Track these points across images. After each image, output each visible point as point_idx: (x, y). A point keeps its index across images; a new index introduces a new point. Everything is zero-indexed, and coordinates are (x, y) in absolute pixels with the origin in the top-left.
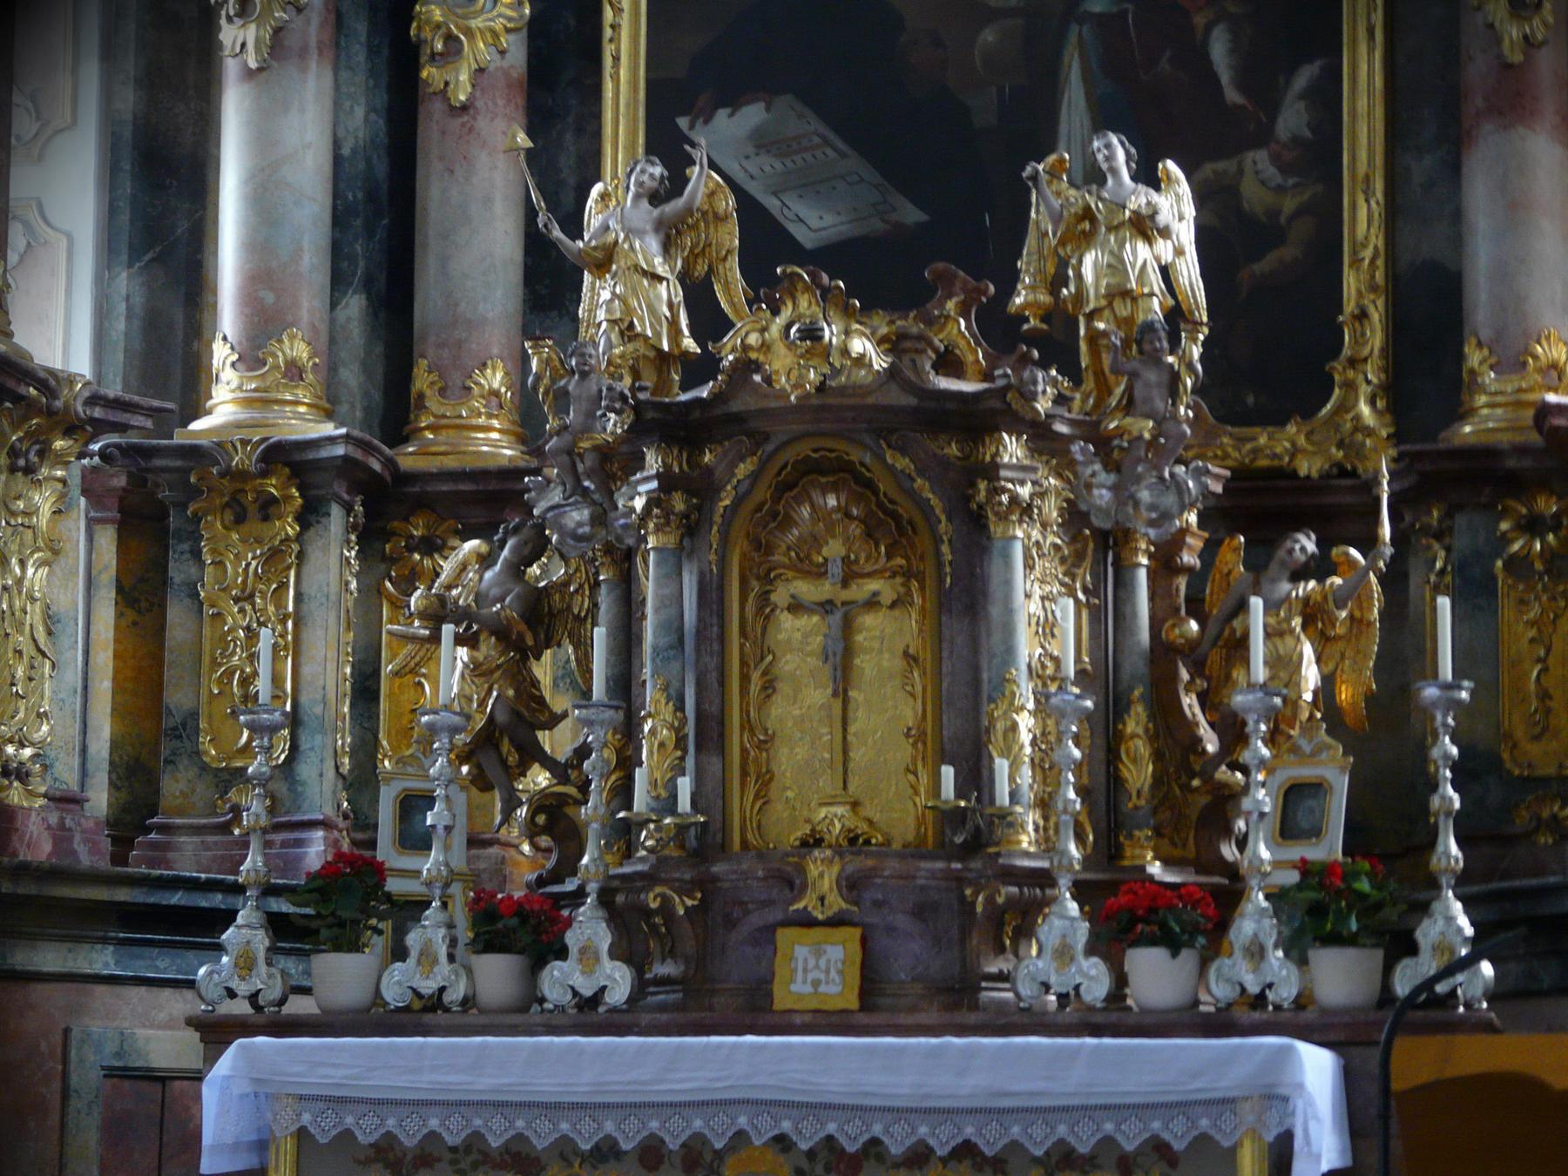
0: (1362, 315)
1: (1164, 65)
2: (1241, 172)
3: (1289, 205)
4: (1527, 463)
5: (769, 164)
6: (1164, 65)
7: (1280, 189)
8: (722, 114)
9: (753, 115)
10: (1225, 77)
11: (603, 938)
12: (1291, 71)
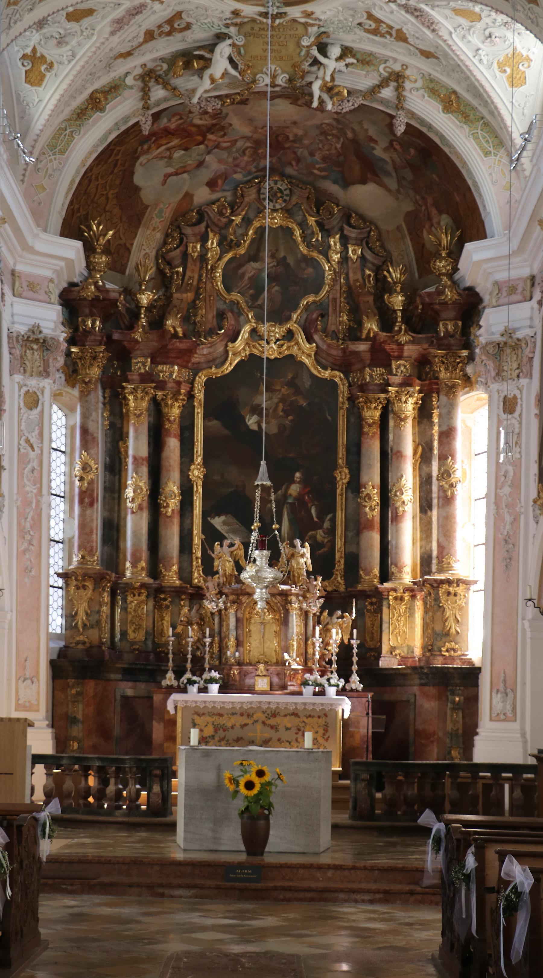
0: (339, 562)
1: (303, 513)
3: (326, 540)
4: (371, 593)
5: (226, 528)
6: (303, 513)
7: (324, 537)
8: (217, 518)
9: (223, 518)
10: (314, 516)
11: (173, 676)
12: (327, 515)
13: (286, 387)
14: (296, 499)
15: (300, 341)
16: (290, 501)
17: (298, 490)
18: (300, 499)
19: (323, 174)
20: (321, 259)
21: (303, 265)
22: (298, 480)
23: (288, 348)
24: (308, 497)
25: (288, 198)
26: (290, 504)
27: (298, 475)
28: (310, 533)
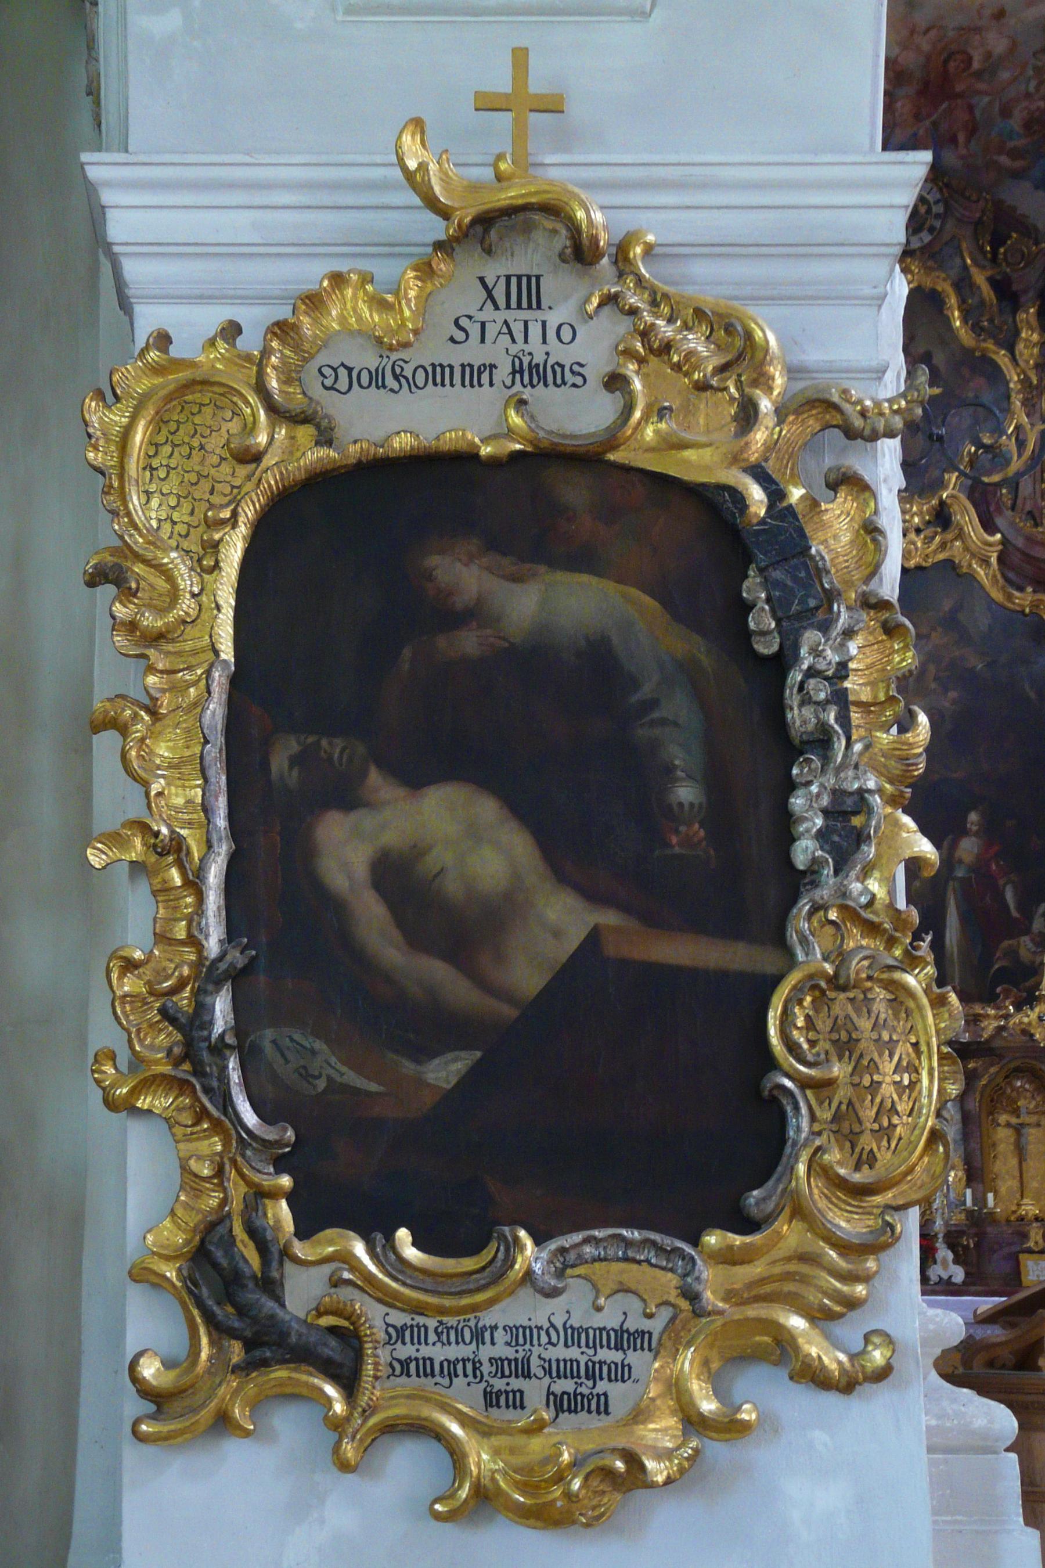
2: (1019, 945)
7: (1035, 953)
13: (940, 630)
14: (973, 869)
15: (968, 529)
16: (960, 873)
17: (976, 851)
18: (979, 869)
19: (1019, 164)
20: (1002, 357)
21: (966, 372)
22: (974, 828)
23: (943, 546)
24: (998, 865)
25: (938, 224)
26: (962, 880)
27: (973, 817)
28: (1006, 944)
